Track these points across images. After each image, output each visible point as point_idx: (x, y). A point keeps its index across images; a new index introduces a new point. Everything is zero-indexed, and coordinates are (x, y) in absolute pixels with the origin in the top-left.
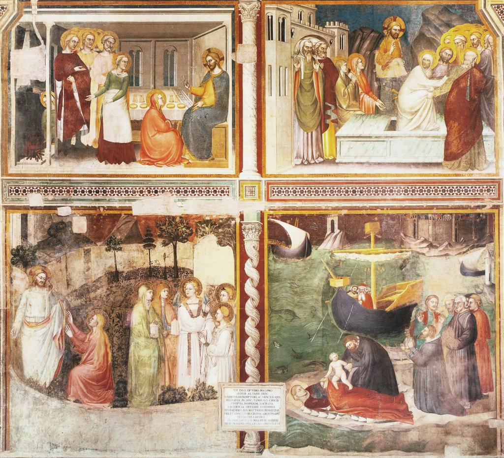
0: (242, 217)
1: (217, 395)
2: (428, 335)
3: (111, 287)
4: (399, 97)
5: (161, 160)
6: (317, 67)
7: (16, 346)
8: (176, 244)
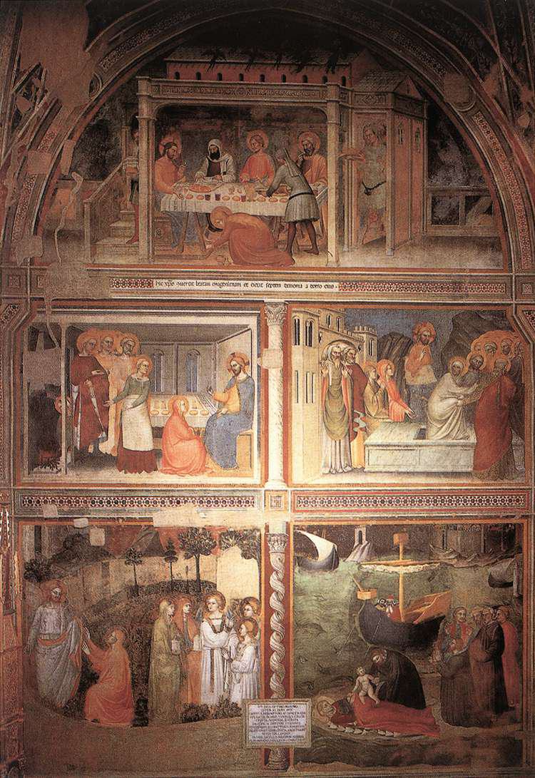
0: (267, 528)
1: (241, 712)
2: (455, 648)
4: (430, 405)
5: (184, 469)
6: (345, 373)
8: (199, 556)
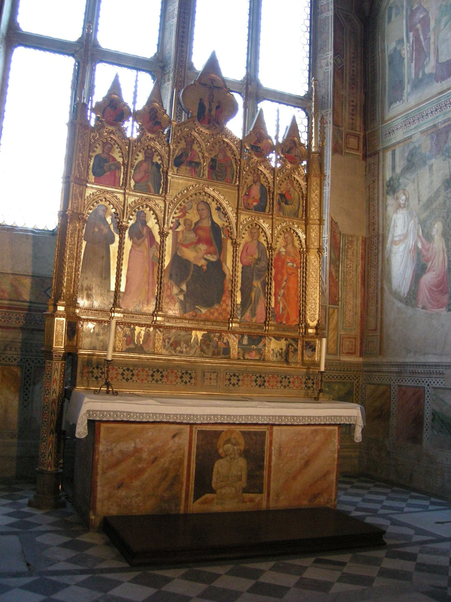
3: (447, 194)
7: (388, 263)
